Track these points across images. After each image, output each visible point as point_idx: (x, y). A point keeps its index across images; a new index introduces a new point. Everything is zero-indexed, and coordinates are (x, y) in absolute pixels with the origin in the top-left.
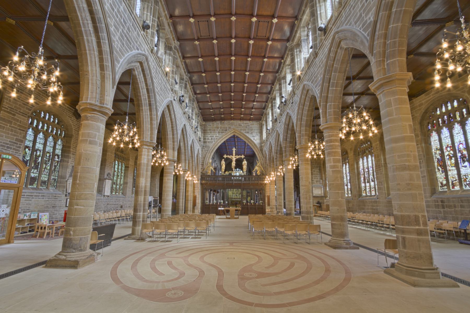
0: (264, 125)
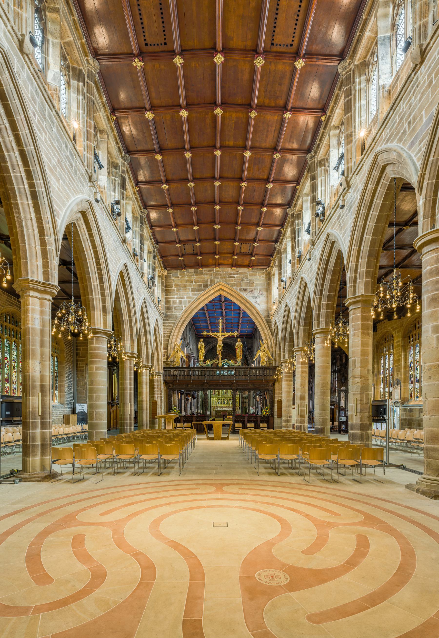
0: (274, 275)
